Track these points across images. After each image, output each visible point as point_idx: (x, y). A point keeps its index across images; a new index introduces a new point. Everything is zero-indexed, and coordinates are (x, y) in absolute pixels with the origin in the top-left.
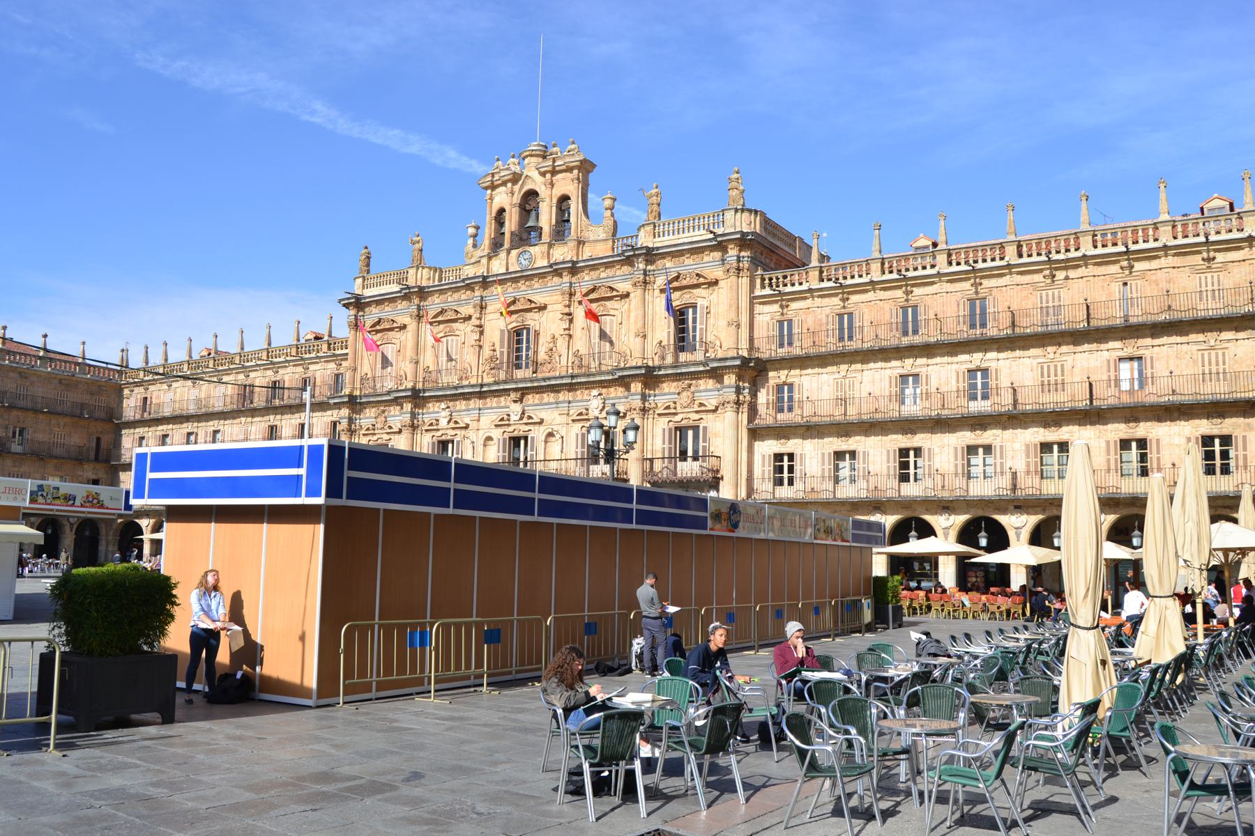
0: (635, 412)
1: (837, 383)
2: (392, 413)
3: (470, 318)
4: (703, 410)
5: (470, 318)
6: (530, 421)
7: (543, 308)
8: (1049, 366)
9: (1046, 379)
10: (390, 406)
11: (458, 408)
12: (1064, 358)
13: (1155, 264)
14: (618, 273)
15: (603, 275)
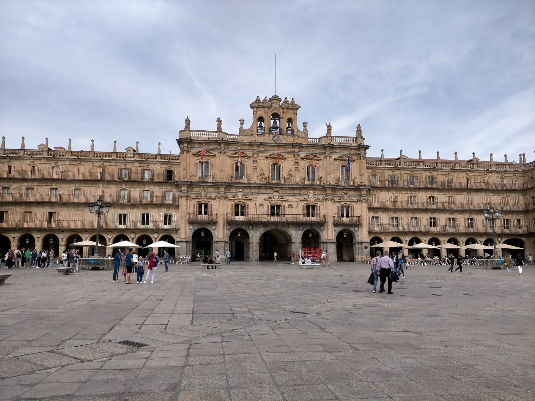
0: (330, 200)
1: (392, 196)
2: (210, 191)
3: (250, 157)
4: (352, 201)
5: (250, 157)
6: (283, 200)
7: (285, 158)
8: (450, 198)
9: (449, 201)
10: (209, 188)
11: (245, 192)
12: (453, 196)
13: (473, 174)
14: (318, 151)
15: (311, 151)
